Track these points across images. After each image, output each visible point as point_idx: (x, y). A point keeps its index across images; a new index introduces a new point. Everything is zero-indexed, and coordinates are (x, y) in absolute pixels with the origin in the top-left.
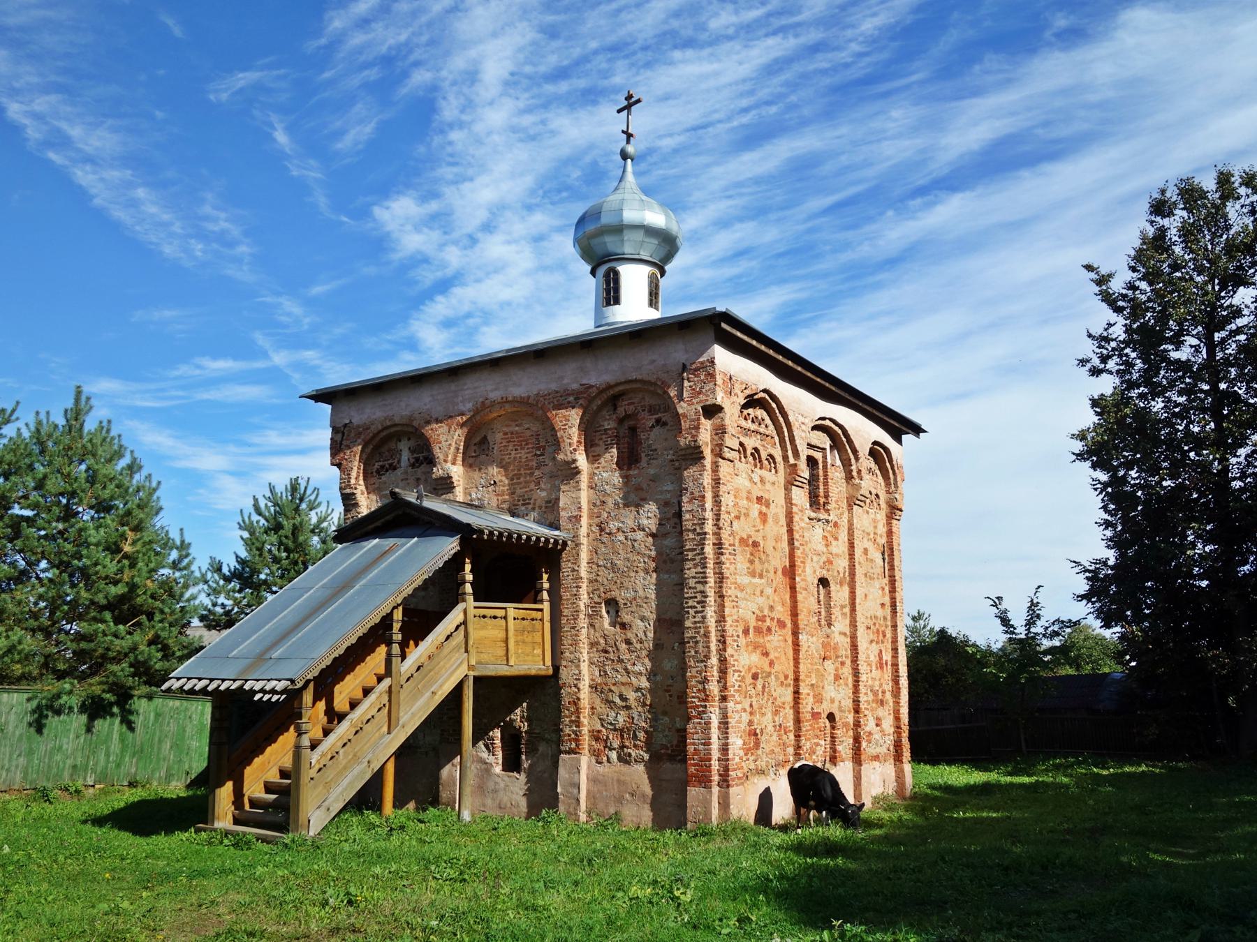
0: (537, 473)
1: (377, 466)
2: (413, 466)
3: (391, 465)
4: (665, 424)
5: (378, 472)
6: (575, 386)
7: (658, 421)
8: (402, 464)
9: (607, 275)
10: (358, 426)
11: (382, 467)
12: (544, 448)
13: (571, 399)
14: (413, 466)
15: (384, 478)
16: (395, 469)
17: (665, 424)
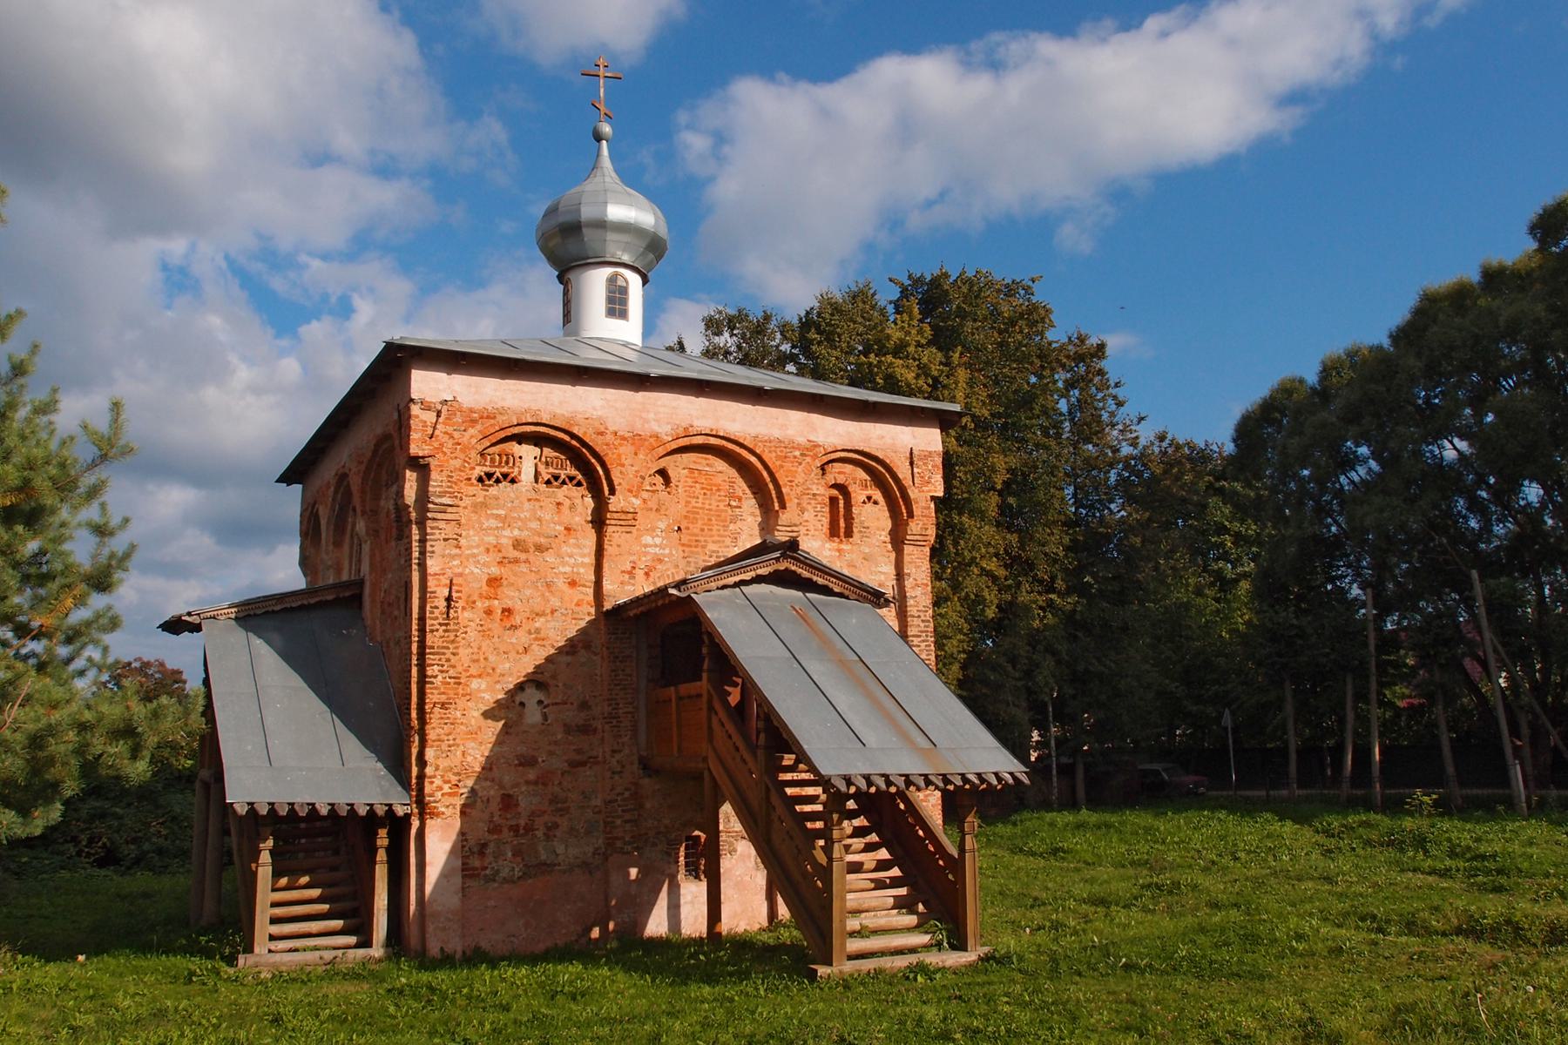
0: (732, 527)
1: (479, 471)
2: (548, 482)
3: (505, 476)
4: (876, 503)
5: (480, 480)
6: (801, 440)
7: (869, 498)
8: (523, 477)
9: (612, 280)
10: (471, 411)
11: (489, 475)
12: (740, 499)
13: (797, 453)
14: (548, 482)
15: (494, 491)
16: (513, 481)
17: (876, 503)
